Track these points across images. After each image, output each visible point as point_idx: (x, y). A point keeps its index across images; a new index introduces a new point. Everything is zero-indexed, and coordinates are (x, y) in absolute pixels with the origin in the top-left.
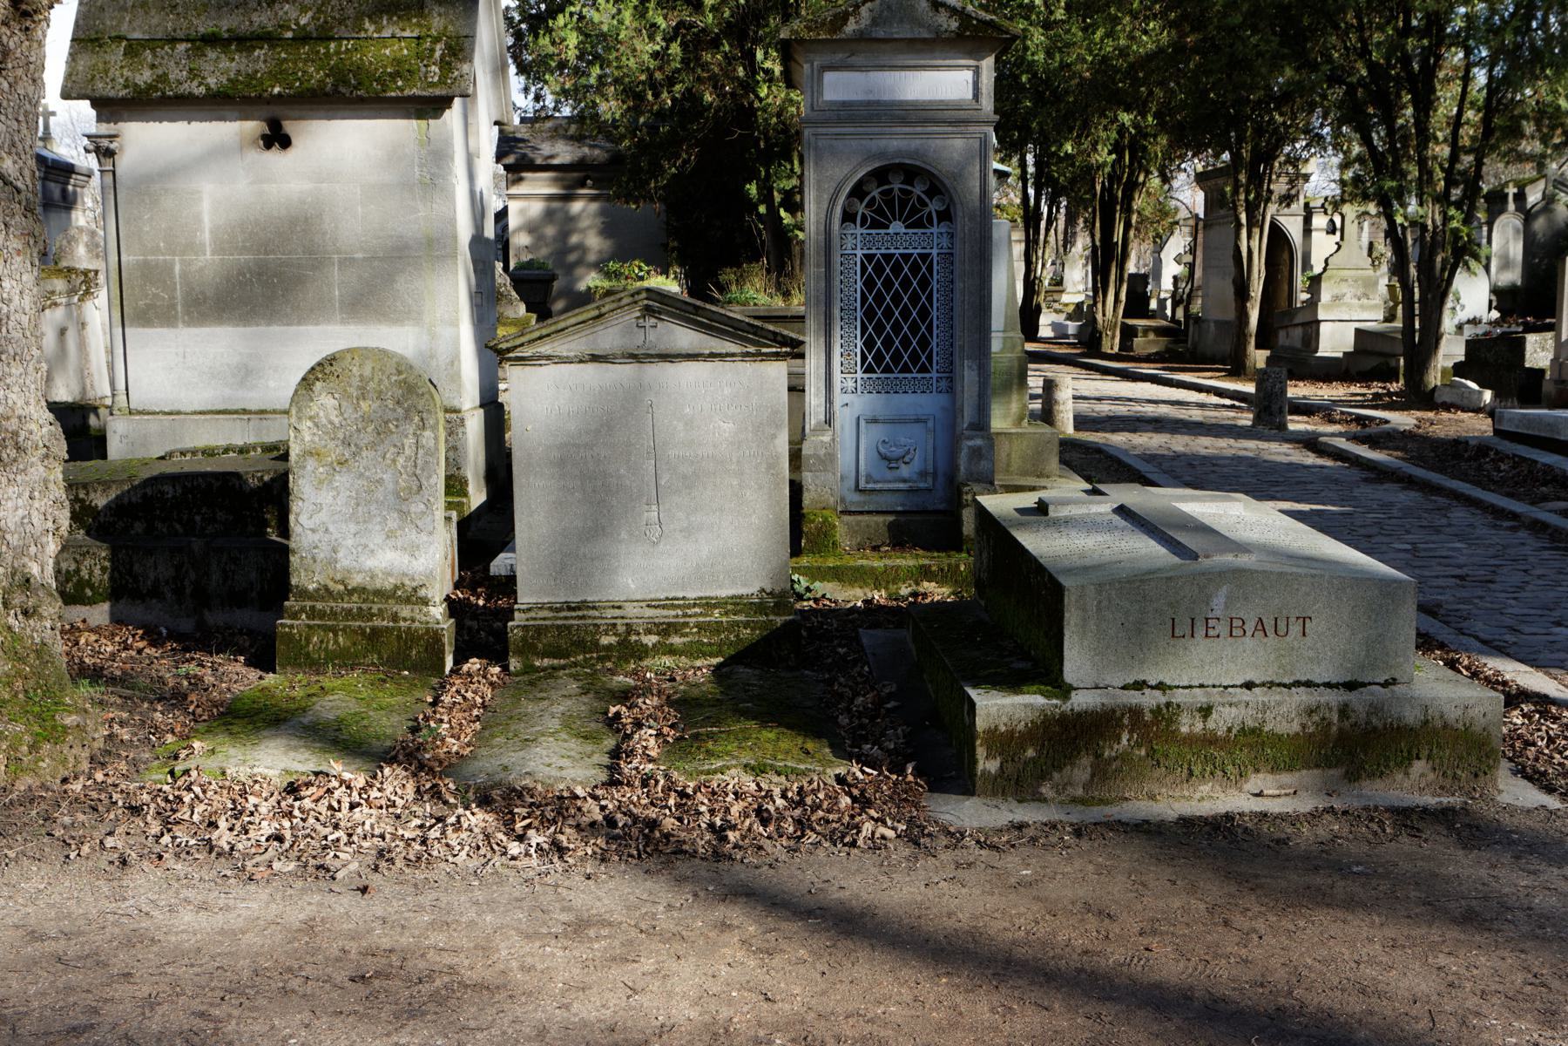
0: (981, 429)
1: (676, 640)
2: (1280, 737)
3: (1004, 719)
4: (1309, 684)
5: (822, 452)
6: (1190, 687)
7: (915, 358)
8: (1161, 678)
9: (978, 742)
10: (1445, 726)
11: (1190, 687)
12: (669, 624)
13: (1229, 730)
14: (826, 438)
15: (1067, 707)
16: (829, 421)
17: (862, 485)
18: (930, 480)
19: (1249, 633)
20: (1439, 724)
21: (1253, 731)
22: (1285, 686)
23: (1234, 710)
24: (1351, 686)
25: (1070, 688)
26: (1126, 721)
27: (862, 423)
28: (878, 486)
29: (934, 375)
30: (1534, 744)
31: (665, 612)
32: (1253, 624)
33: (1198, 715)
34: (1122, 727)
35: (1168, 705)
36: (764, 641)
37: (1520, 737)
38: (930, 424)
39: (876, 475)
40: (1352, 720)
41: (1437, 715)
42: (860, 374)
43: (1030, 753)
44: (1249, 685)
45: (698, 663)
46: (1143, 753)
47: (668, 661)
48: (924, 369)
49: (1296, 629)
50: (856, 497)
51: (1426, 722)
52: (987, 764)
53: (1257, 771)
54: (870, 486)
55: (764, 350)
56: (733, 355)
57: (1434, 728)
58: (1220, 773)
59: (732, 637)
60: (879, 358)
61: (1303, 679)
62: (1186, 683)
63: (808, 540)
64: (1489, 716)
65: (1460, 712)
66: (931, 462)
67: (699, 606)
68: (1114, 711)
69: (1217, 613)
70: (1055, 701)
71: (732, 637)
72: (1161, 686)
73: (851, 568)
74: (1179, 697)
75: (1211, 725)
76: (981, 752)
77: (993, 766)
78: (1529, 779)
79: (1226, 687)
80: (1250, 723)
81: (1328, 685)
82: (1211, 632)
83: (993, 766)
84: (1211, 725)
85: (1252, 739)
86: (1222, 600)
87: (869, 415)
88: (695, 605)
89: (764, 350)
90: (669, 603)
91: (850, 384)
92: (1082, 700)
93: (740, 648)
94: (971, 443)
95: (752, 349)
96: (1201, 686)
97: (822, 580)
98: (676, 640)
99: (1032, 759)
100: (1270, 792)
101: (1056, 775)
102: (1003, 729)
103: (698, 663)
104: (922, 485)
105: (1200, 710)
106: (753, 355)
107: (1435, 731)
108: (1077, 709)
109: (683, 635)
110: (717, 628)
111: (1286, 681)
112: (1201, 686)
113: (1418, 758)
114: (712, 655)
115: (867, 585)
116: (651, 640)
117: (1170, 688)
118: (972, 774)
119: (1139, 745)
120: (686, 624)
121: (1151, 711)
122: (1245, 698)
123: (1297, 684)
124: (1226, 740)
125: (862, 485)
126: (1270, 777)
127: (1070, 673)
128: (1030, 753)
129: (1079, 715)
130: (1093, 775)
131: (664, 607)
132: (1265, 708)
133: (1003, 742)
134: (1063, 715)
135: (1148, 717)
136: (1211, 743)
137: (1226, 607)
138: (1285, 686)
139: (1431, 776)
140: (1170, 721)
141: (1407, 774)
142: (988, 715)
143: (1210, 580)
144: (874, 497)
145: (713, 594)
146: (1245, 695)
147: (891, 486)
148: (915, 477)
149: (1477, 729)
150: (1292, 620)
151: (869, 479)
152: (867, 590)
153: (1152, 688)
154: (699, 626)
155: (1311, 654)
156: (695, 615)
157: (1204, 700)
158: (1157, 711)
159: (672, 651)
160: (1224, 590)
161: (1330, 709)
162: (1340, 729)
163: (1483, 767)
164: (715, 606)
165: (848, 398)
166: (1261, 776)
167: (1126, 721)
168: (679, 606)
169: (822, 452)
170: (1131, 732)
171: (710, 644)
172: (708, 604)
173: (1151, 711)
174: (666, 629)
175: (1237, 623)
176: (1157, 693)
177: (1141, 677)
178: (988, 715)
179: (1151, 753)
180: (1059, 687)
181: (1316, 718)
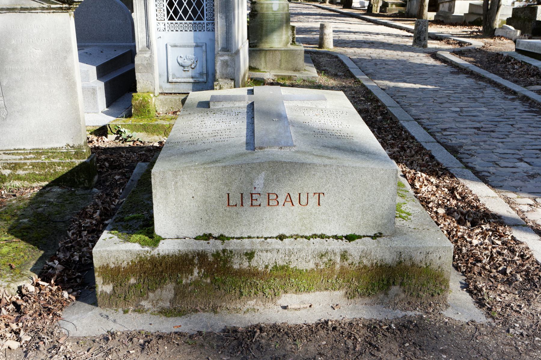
0: (228, 51)
1: (20, 172)
2: (301, 272)
3: (113, 260)
4: (322, 237)
5: (145, 63)
6: (242, 238)
7: (194, 12)
8: (221, 232)
9: (96, 274)
10: (413, 265)
11: (242, 238)
12: (16, 164)
13: (267, 267)
14: (147, 55)
15: (155, 252)
16: (149, 46)
17: (170, 80)
18: (205, 77)
19: (281, 203)
20: (409, 264)
21: (283, 268)
22: (306, 237)
23: (269, 254)
24: (350, 238)
25: (160, 239)
26: (196, 261)
27: (169, 47)
28: (178, 80)
29: (205, 21)
30: (481, 261)
31: (14, 157)
32: (284, 197)
33: (245, 257)
34: (193, 265)
35: (224, 251)
36: (70, 173)
37: (473, 255)
38: (204, 48)
39: (178, 75)
40: (350, 261)
41: (408, 258)
42: (167, 21)
43: (132, 281)
44: (281, 237)
45: (34, 185)
46: (209, 281)
47: (17, 183)
48: (199, 19)
49: (313, 200)
50: (169, 86)
51: (400, 262)
52: (103, 287)
53: (286, 292)
54: (174, 80)
55: (53, 6)
56: (35, 9)
57: (405, 266)
58: (260, 293)
59: (52, 171)
60: (176, 12)
61: (319, 233)
62: (239, 236)
63: (136, 109)
64: (443, 259)
65: (423, 256)
66: (205, 68)
67: (33, 153)
68: (187, 255)
69: (259, 190)
70: (147, 248)
71: (52, 171)
72: (222, 238)
73: (152, 125)
74: (232, 245)
75: (254, 263)
76: (99, 280)
77: (108, 289)
78: (470, 292)
79: (266, 238)
80: (281, 263)
81: (336, 237)
82: (255, 203)
83: (108, 289)
84: (254, 263)
85: (281, 273)
86: (262, 182)
87: (173, 43)
88: (30, 153)
89: (53, 6)
90: (16, 152)
91: (162, 27)
92: (166, 248)
93: (57, 177)
94: (222, 58)
95: (46, 5)
96: (249, 237)
97: (137, 131)
98: (20, 172)
99: (134, 285)
100: (293, 307)
101: (151, 295)
102: (112, 266)
103: (34, 185)
104: (201, 80)
105: (246, 254)
106: (47, 9)
107: (406, 269)
108: (162, 253)
109: (24, 170)
110: (43, 166)
111: (308, 234)
112: (249, 237)
113: (394, 284)
114: (41, 180)
115: (160, 134)
116: (7, 172)
117: (228, 238)
118: (94, 293)
119: (206, 276)
120: (25, 164)
121: (213, 255)
122: (277, 247)
123: (315, 236)
124: (265, 273)
125: (170, 80)
126: (294, 296)
127: (159, 228)
128: (132, 281)
129: (164, 257)
130: (176, 295)
131: (13, 154)
132: (290, 253)
133: (114, 274)
134: (152, 257)
135: (211, 259)
136: (254, 275)
137: (265, 186)
138: (306, 237)
139: (403, 296)
140: (226, 261)
141: (386, 294)
142: (101, 257)
143: (252, 168)
144: (177, 85)
145: (40, 147)
146: (277, 244)
147: (183, 80)
148: (197, 75)
149: (434, 266)
150: (311, 195)
151: (174, 76)
152: (161, 137)
153: (216, 238)
154: (34, 165)
155: (324, 217)
156: (31, 159)
157: (249, 248)
158: (216, 255)
159: (19, 178)
160: (263, 175)
161: (335, 254)
162: (342, 267)
163: (438, 291)
164: (42, 154)
165: (162, 34)
166: (288, 295)
167: (196, 261)
168: (21, 154)
169: (145, 63)
170: (200, 268)
171: (40, 175)
172: (38, 153)
173: (213, 255)
174: (15, 166)
175: (273, 197)
176: (218, 242)
177: (208, 232)
178: (101, 257)
179: (214, 281)
180: (152, 237)
181: (325, 259)
